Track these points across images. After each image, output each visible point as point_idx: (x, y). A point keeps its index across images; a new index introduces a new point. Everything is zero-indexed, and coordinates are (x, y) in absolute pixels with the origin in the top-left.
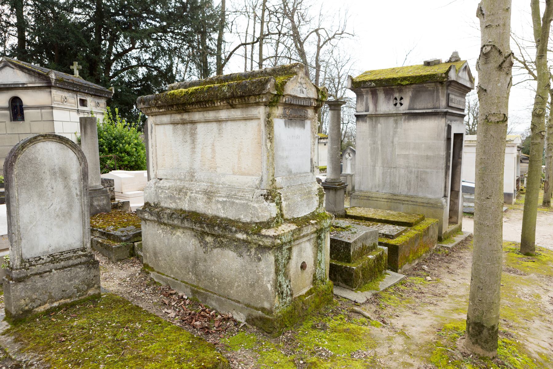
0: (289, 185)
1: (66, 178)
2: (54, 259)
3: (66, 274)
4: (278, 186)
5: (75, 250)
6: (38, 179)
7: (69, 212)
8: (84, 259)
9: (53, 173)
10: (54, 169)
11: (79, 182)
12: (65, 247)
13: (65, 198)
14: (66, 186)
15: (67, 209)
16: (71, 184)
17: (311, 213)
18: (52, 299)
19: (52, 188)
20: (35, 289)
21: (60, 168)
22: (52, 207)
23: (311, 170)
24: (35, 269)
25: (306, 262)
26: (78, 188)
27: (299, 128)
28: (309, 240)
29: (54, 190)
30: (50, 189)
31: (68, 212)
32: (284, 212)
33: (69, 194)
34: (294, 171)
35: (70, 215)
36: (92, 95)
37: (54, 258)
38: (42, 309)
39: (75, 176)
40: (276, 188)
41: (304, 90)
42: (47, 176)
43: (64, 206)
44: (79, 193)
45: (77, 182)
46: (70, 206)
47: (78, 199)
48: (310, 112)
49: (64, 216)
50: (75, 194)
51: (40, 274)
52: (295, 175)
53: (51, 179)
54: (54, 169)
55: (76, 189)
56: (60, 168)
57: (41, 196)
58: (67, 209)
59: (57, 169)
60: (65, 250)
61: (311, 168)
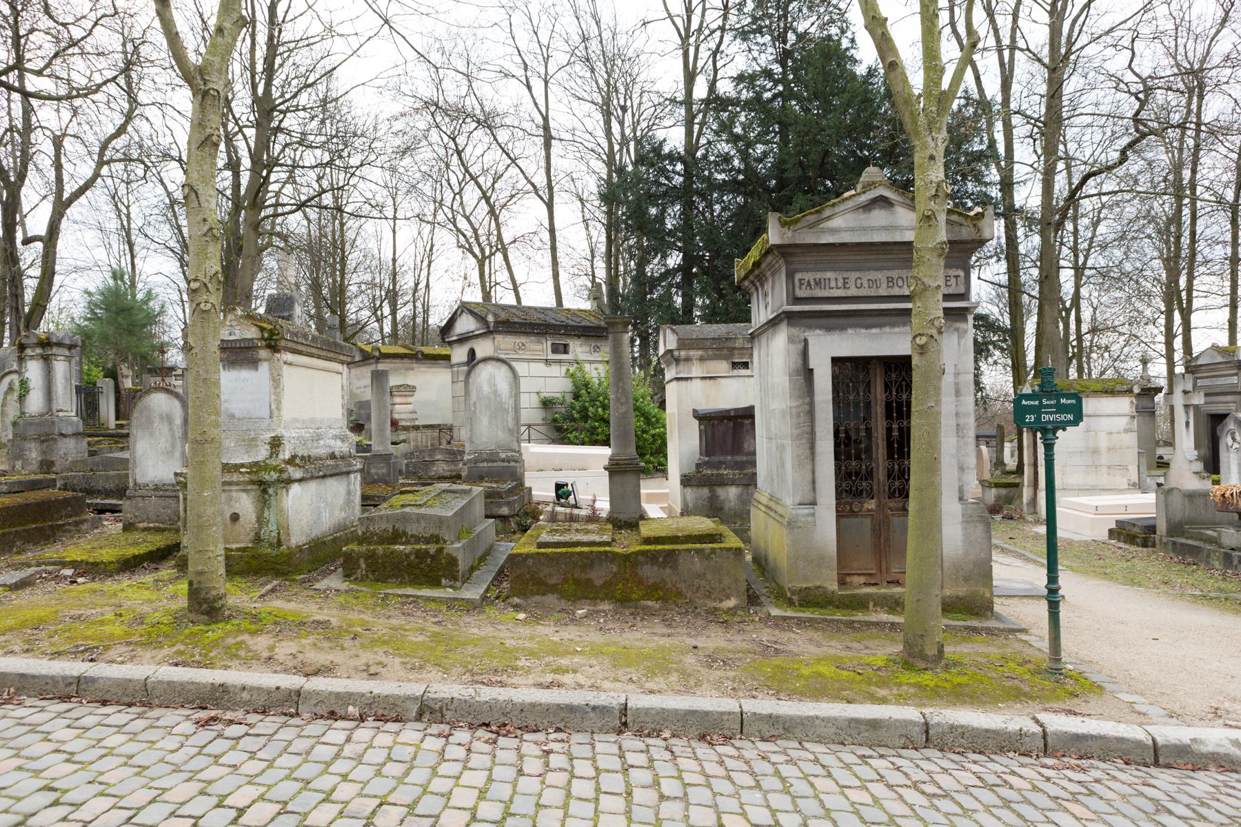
2: (157, 488)
3: (162, 502)
6: (150, 422)
9: (162, 418)
18: (149, 520)
20: (138, 509)
24: (141, 492)
33: (173, 436)
34: (237, 415)
36: (579, 337)
38: (141, 525)
39: (178, 421)
42: (157, 420)
46: (173, 446)
48: (263, 353)
51: (143, 497)
52: (239, 419)
57: (151, 435)
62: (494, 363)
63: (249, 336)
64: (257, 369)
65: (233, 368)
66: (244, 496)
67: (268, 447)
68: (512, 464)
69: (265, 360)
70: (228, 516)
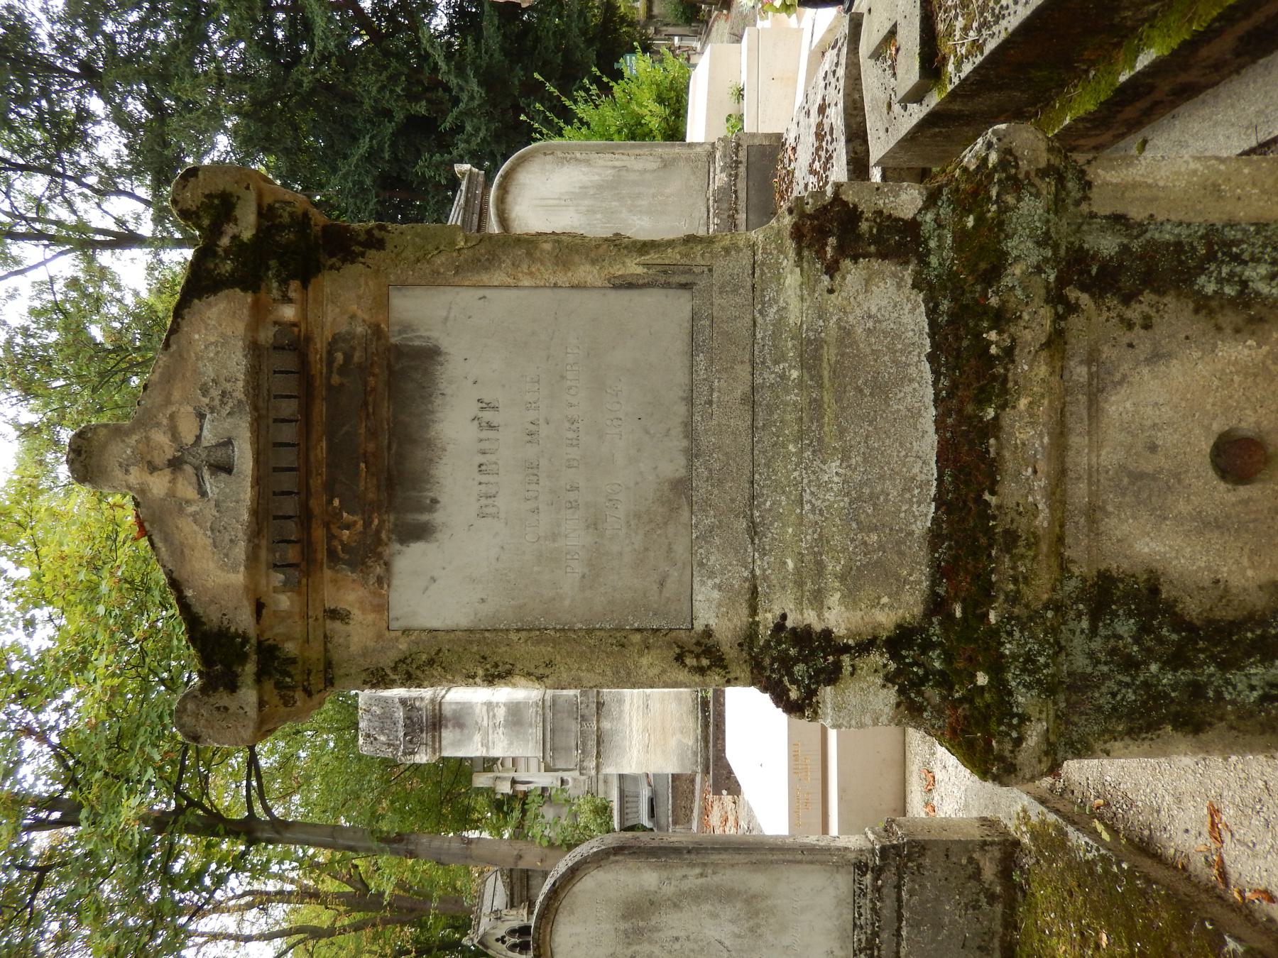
0: (743, 524)
1: (652, 903)
4: (741, 617)
5: (858, 891)
7: (746, 900)
8: (890, 876)
10: (626, 932)
11: (665, 867)
12: (841, 915)
13: (707, 907)
14: (675, 905)
15: (739, 905)
16: (669, 890)
17: (932, 358)
19: (677, 939)
21: (624, 917)
22: (727, 943)
23: (684, 286)
25: (1218, 427)
26: (685, 871)
27: (438, 401)
28: (1095, 394)
29: (683, 934)
30: (677, 946)
31: (748, 902)
32: (885, 619)
33: (696, 897)
34: (674, 467)
35: (754, 896)
37: (865, 948)
40: (750, 636)
41: (209, 437)
43: (727, 912)
44: (697, 871)
45: (665, 874)
46: (727, 895)
47: (714, 873)
49: (757, 914)
50: (701, 881)
52: (692, 454)
53: (651, 942)
54: (626, 932)
55: (685, 876)
56: (624, 917)
58: (739, 905)
59: (623, 926)
60: (851, 917)
61: (667, 285)
62: (510, 198)
63: (236, 363)
64: (429, 355)
65: (421, 479)
66: (1117, 406)
67: (853, 274)
68: (743, 155)
69: (382, 303)
70: (1224, 495)
